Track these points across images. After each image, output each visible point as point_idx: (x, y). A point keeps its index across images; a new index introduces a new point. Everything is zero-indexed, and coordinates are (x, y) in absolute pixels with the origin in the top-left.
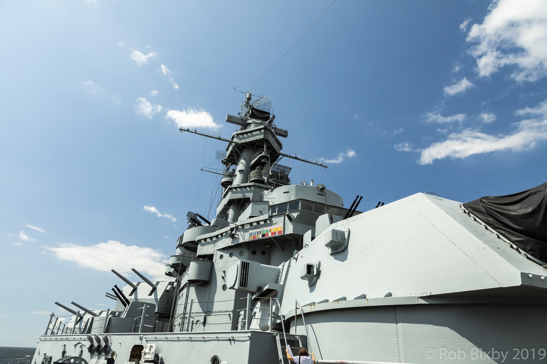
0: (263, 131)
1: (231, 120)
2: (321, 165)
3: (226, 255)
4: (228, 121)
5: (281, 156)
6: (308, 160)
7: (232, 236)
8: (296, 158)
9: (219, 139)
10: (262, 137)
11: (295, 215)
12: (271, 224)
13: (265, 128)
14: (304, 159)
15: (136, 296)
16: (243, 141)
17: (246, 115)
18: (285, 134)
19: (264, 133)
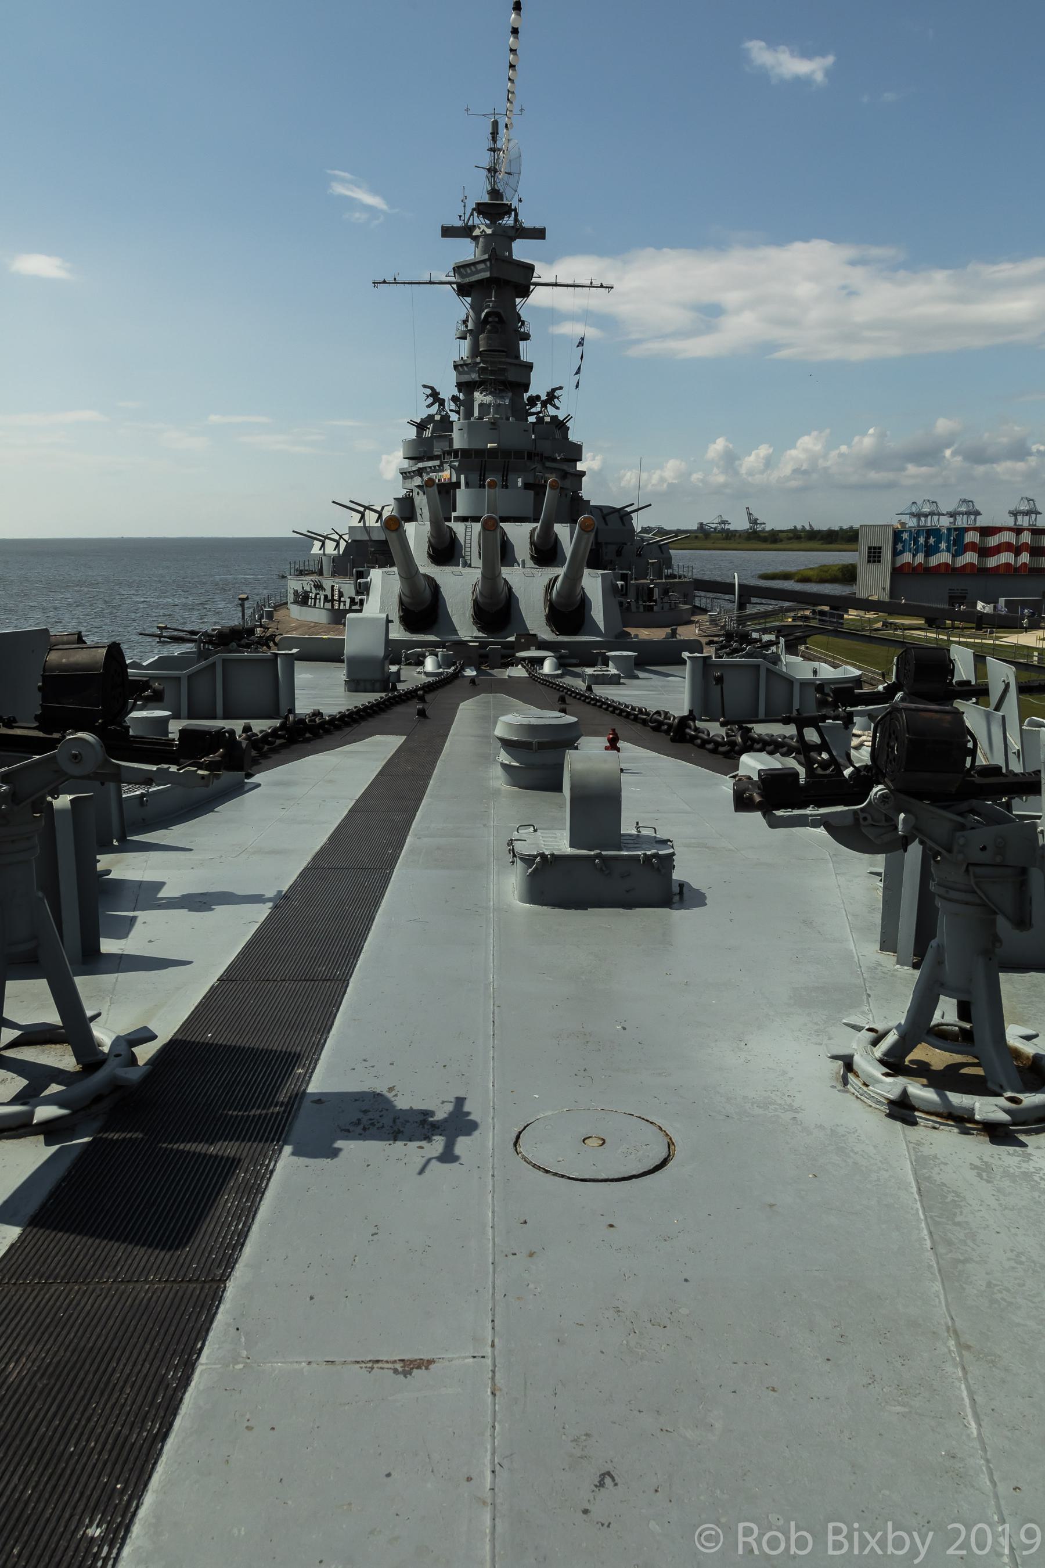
0: (488, 263)
1: (448, 232)
2: (602, 286)
3: (421, 493)
4: (443, 236)
5: (532, 287)
6: (577, 282)
7: (421, 476)
8: (556, 285)
9: (431, 283)
10: (487, 274)
11: (456, 464)
12: (443, 471)
13: (489, 259)
14: (571, 282)
15: (364, 523)
16: (467, 280)
17: (472, 214)
18: (539, 234)
19: (491, 269)
